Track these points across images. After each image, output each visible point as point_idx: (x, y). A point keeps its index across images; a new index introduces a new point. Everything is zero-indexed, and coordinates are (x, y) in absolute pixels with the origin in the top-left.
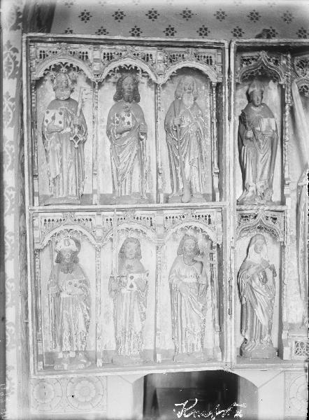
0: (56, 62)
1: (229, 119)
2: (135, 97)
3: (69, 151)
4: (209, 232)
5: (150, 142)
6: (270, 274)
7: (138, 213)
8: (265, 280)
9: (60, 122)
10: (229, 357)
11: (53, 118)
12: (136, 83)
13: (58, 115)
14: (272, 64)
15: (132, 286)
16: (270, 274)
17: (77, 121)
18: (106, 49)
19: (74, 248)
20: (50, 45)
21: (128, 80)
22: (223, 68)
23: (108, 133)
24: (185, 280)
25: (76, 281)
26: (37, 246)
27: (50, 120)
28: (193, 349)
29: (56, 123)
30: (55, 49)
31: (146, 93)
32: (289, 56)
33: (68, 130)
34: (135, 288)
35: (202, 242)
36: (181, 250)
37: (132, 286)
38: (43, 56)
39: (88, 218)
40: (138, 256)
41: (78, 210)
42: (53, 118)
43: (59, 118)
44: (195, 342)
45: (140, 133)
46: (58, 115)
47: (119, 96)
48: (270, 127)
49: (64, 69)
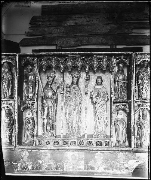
1: (16, 75)
6: (31, 121)
16: (31, 121)
48: (31, 78)
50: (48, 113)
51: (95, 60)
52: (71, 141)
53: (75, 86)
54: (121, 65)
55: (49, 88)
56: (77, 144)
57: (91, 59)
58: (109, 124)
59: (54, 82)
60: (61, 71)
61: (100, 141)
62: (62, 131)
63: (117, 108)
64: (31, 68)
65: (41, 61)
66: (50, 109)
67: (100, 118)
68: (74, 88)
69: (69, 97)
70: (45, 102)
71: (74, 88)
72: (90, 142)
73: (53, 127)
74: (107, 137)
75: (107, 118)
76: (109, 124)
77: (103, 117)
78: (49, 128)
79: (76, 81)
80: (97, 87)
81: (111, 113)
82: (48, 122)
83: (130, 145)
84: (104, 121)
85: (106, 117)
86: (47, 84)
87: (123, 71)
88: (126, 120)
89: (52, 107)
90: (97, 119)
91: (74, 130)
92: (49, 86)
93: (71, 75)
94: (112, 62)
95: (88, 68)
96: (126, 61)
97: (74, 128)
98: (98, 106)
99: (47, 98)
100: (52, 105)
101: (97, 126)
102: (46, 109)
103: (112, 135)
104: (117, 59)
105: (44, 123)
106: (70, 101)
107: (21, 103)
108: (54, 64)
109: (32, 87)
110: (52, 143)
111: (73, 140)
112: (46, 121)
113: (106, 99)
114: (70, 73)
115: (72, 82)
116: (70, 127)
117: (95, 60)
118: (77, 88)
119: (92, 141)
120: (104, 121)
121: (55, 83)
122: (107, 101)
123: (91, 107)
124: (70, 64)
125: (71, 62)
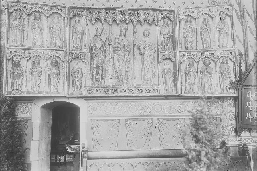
0: (16, 8)
1: (67, 26)
2: (40, 19)
3: (19, 32)
4: (60, 57)
5: (44, 32)
7: (39, 51)
8: (78, 73)
9: (17, 24)
10: (65, 93)
11: (15, 23)
12: (40, 16)
13: (16, 22)
14: (80, 12)
15: (36, 71)
16: (80, 71)
17: (22, 24)
18: (32, 6)
19: (20, 60)
20: (15, 3)
21: (38, 14)
22: (65, 12)
23: (31, 29)
24: (52, 71)
25: (19, 69)
26: (8, 58)
27: (14, 24)
28: (54, 91)
29: (16, 24)
30: (16, 5)
31: (44, 19)
32: (86, 11)
33: (19, 27)
34: (37, 72)
35: (58, 60)
36: (52, 63)
37: (36, 71)
38: (13, 6)
39: (24, 51)
40: (39, 63)
41: (21, 49)
42: (15, 23)
43: (16, 23)
44: (54, 89)
45: (41, 30)
46: (16, 22)
47: (35, 19)
49: (19, 10)
50: (98, 63)
51: (142, 14)
52: (122, 88)
53: (123, 37)
54: (166, 20)
55: (98, 39)
56: (127, 92)
57: (138, 14)
58: (157, 74)
59: (103, 33)
60: (110, 23)
61: (149, 88)
62: (111, 81)
63: (163, 57)
64: (79, 19)
65: (90, 13)
66: (99, 59)
67: (148, 67)
68: (123, 39)
69: (119, 47)
70: (94, 52)
71: (123, 39)
72: (139, 90)
73: (103, 78)
74: (156, 85)
75: (154, 68)
76: (157, 74)
77: (151, 67)
78: (99, 77)
79: (124, 33)
80: (145, 39)
81: (158, 63)
82: (97, 74)
83: (177, 92)
84: (153, 71)
85: (154, 66)
86: (96, 35)
87: (167, 24)
88: (173, 71)
89: (102, 57)
90: (146, 69)
91: (124, 79)
92: (98, 37)
93: (119, 27)
94: (158, 16)
95: (135, 21)
96: (170, 16)
97: (123, 77)
98: (146, 56)
99: (96, 48)
100: (101, 55)
101: (145, 76)
102: (95, 59)
103: (159, 83)
104: (162, 14)
105: (93, 72)
106: (119, 51)
107: (70, 52)
108: (103, 16)
109: (80, 38)
110: (102, 91)
111: (124, 88)
112: (95, 71)
113: (153, 50)
114: (118, 25)
115: (121, 35)
116: (120, 76)
117: (142, 14)
118: (125, 40)
119: (141, 89)
120: (153, 71)
121: (104, 34)
122: (154, 52)
123: (138, 57)
124: (118, 18)
125: (120, 15)
